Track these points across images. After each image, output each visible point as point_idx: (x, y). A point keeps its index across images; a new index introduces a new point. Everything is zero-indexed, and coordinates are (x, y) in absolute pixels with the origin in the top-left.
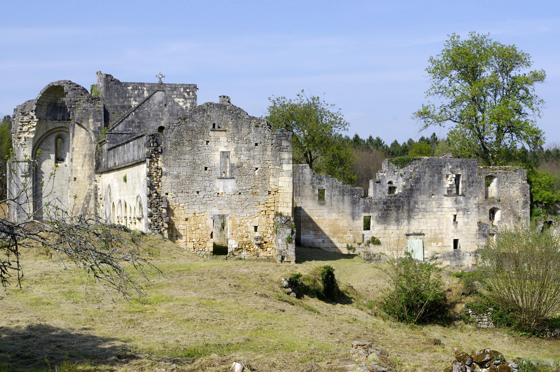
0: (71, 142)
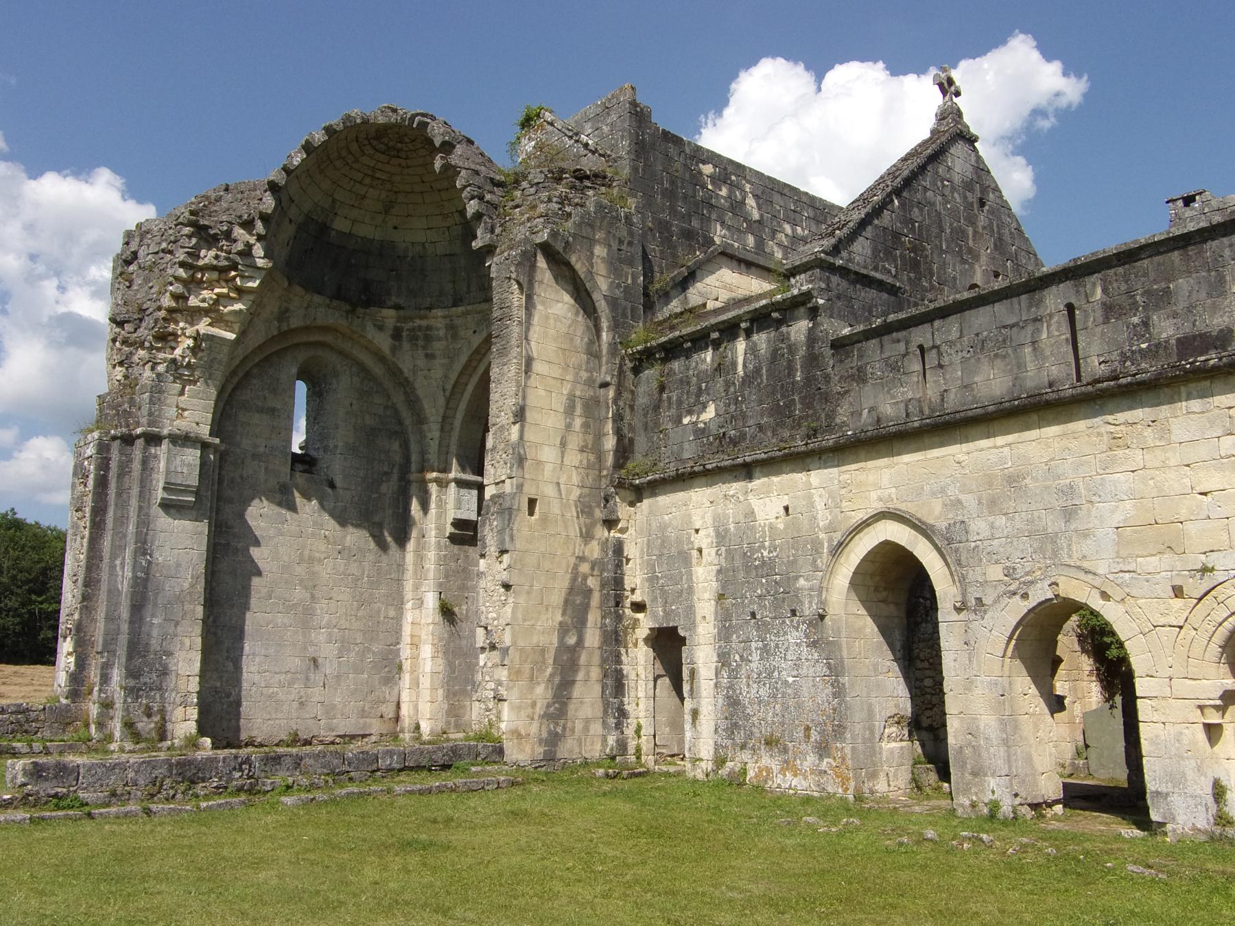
0: (515, 330)
